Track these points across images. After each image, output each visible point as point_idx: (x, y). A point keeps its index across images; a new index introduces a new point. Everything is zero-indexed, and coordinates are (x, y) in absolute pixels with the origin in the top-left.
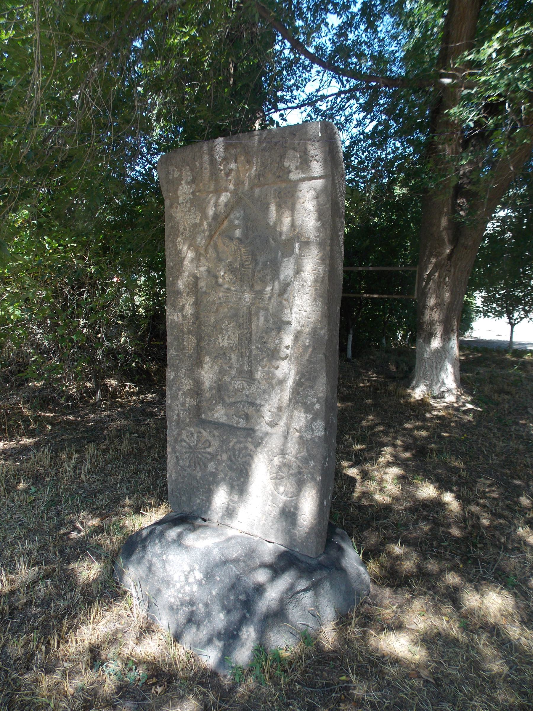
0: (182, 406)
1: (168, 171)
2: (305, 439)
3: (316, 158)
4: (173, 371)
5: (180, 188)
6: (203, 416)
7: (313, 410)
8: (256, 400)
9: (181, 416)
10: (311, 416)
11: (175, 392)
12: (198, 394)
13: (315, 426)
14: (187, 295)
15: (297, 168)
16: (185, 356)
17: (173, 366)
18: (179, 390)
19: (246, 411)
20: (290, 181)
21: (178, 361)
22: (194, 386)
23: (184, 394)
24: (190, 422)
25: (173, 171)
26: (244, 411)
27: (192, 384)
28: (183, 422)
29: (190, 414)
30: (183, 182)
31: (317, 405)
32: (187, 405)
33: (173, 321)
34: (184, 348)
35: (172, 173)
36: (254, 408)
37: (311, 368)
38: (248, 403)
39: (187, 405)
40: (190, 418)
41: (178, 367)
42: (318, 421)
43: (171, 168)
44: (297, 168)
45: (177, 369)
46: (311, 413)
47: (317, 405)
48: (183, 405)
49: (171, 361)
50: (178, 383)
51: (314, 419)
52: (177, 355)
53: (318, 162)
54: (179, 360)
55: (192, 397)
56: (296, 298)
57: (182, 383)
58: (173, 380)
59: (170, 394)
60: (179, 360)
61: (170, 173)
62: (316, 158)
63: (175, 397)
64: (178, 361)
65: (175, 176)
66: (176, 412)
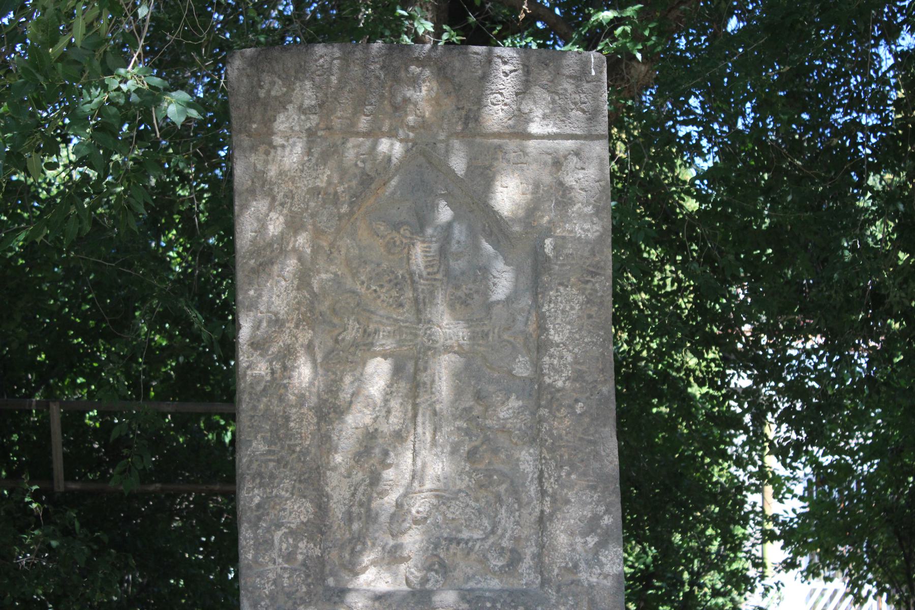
0: (287, 561)
1: (259, 81)
2: (586, 584)
3: (583, 106)
4: (261, 485)
5: (281, 117)
6: (331, 582)
7: (599, 526)
8: (460, 531)
9: (286, 582)
10: (596, 539)
11: (268, 530)
12: (322, 533)
13: (606, 557)
14: (297, 326)
15: (545, 117)
16: (294, 452)
17: (260, 475)
18: (279, 526)
19: (442, 556)
20: (530, 136)
21: (271, 465)
22: (315, 514)
23: (292, 532)
24: (308, 593)
25: (273, 83)
26: (437, 556)
27: (311, 510)
28: (289, 595)
29: (308, 576)
30: (290, 107)
31: (606, 517)
32: (300, 557)
33: (258, 379)
34: (289, 436)
35: (267, 86)
36: (462, 545)
37: (590, 453)
38: (446, 539)
39: (300, 557)
40: (308, 585)
41: (272, 477)
42: (611, 546)
43: (267, 78)
44: (545, 117)
45: (266, 480)
46: (596, 534)
47: (606, 517)
48: (289, 557)
49: (255, 466)
50: (273, 513)
51: (602, 544)
52: (269, 452)
53: (584, 112)
54: (278, 461)
55: (311, 539)
56: (552, 332)
57: (284, 510)
58: (259, 506)
59: (255, 538)
60: (278, 461)
61: (261, 87)
62: (583, 106)
63: (265, 544)
64: (271, 465)
65: (273, 93)
66: (272, 576)
